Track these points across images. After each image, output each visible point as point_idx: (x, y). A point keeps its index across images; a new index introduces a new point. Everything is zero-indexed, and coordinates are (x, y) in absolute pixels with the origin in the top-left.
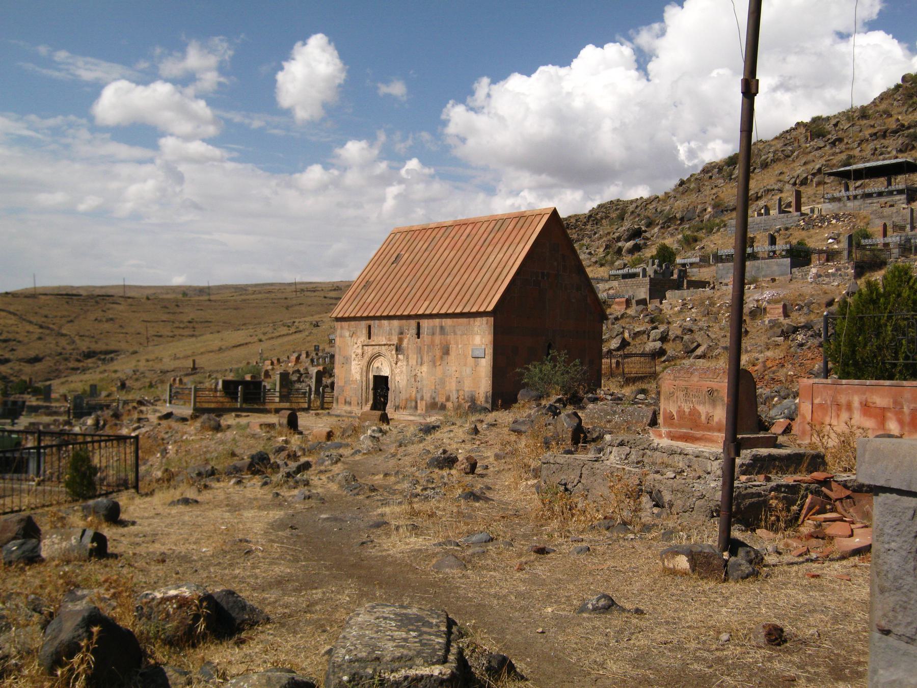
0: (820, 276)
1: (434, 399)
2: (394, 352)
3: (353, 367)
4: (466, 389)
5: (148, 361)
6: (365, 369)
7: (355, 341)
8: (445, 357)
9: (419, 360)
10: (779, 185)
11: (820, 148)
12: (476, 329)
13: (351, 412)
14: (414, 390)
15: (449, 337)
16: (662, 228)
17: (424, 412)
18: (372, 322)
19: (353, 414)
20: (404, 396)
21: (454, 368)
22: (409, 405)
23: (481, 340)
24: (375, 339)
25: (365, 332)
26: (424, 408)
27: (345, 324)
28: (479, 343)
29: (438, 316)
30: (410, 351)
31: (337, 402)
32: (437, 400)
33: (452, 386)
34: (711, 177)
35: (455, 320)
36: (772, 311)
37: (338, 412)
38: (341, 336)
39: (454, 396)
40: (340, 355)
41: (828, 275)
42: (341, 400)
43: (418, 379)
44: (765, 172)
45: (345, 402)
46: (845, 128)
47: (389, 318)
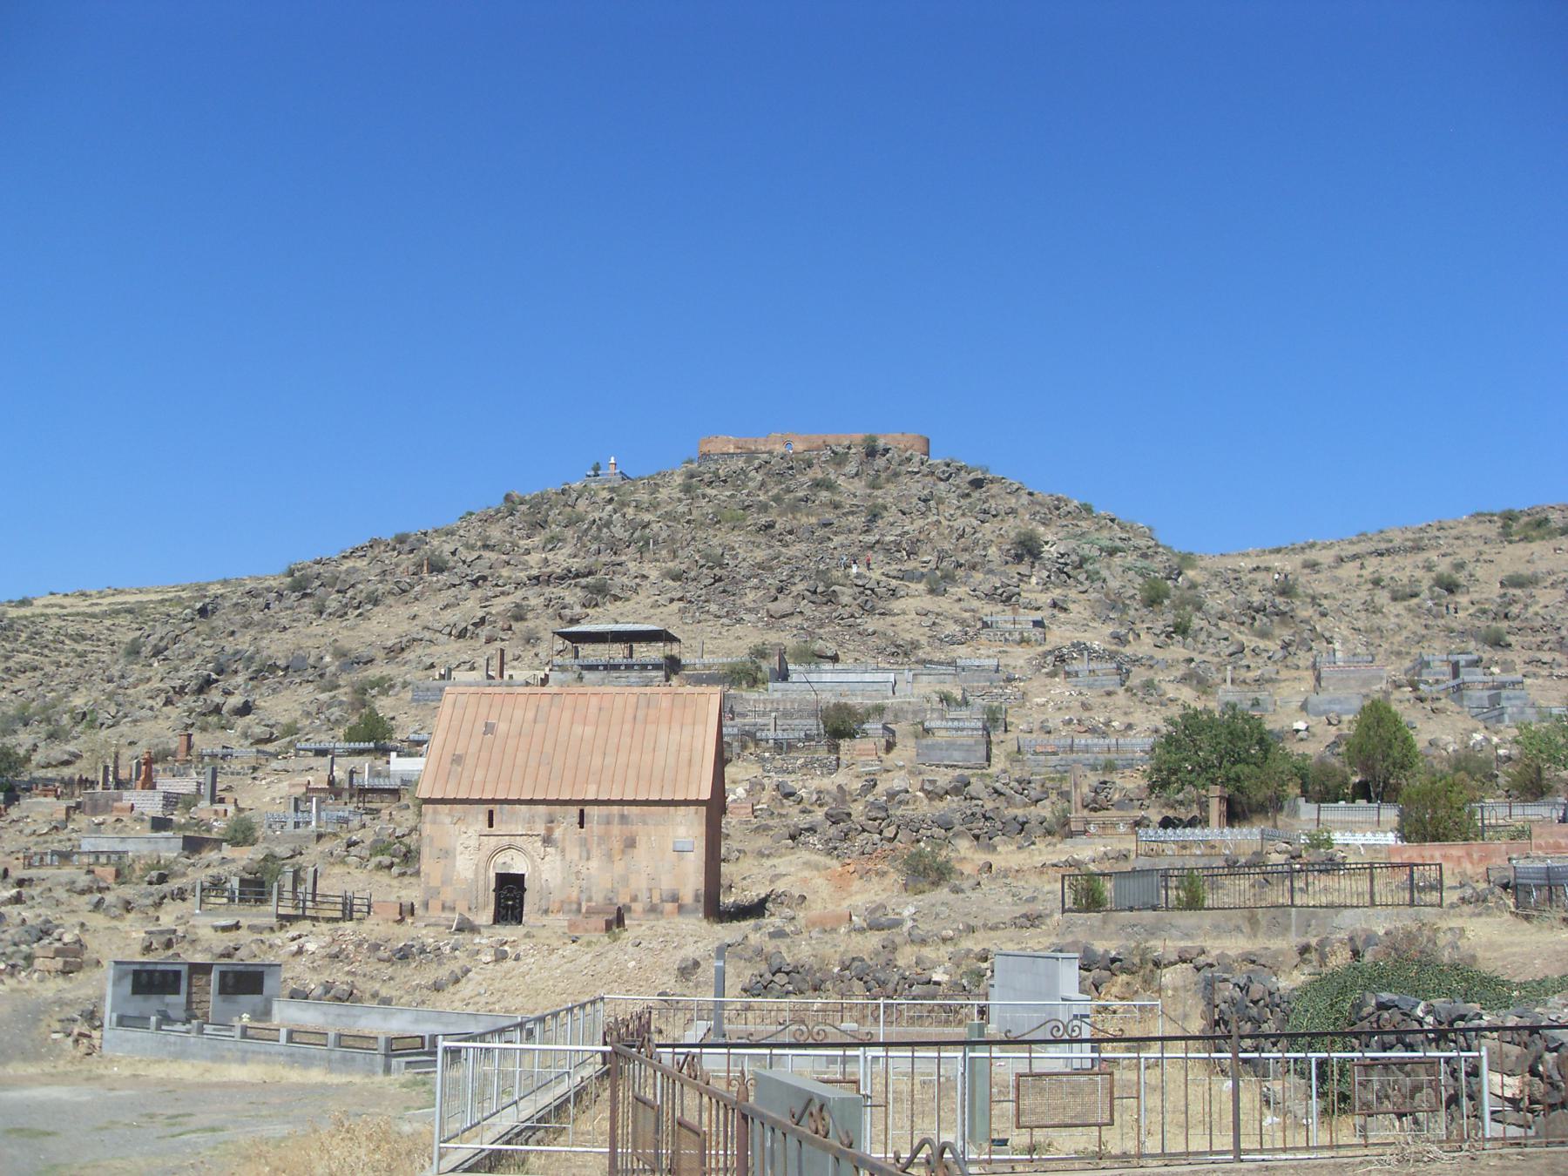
3: (457, 864)
6: (482, 864)
7: (464, 829)
8: (630, 850)
9: (584, 855)
10: (427, 635)
11: (454, 586)
12: (679, 819)
16: (251, 679)
20: (557, 897)
22: (566, 907)
25: (484, 818)
27: (445, 808)
29: (622, 803)
34: (267, 606)
36: (737, 811)
38: (434, 822)
39: (643, 896)
44: (376, 609)
45: (444, 908)
46: (469, 560)
47: (531, 802)
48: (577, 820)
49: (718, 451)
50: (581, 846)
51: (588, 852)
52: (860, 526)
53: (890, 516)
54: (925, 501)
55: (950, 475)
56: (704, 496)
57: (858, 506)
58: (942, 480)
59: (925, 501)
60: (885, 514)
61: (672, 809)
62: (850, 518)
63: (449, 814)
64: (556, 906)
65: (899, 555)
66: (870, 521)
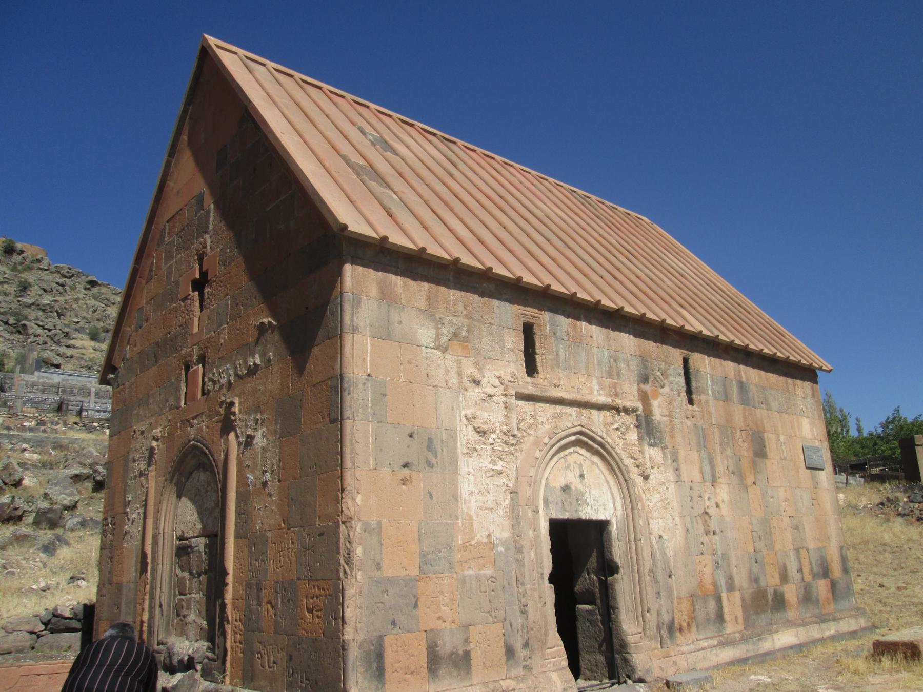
1: (756, 580)
2: (633, 436)
3: (466, 486)
4: (812, 545)
9: (707, 469)
14: (708, 559)
15: (758, 411)
17: (741, 627)
20: (682, 585)
21: (782, 494)
22: (700, 615)
26: (740, 620)
30: (679, 439)
33: (785, 540)
35: (763, 373)
38: (384, 333)
40: (380, 421)
43: (713, 525)
48: (681, 380)
51: (711, 462)
52: (12, 292)
53: (35, 291)
54: (62, 285)
55: (73, 276)
57: (11, 280)
58: (66, 277)
59: (62, 285)
60: (31, 289)
61: (789, 380)
62: (6, 286)
63: (429, 313)
65: (52, 314)
66: (21, 290)
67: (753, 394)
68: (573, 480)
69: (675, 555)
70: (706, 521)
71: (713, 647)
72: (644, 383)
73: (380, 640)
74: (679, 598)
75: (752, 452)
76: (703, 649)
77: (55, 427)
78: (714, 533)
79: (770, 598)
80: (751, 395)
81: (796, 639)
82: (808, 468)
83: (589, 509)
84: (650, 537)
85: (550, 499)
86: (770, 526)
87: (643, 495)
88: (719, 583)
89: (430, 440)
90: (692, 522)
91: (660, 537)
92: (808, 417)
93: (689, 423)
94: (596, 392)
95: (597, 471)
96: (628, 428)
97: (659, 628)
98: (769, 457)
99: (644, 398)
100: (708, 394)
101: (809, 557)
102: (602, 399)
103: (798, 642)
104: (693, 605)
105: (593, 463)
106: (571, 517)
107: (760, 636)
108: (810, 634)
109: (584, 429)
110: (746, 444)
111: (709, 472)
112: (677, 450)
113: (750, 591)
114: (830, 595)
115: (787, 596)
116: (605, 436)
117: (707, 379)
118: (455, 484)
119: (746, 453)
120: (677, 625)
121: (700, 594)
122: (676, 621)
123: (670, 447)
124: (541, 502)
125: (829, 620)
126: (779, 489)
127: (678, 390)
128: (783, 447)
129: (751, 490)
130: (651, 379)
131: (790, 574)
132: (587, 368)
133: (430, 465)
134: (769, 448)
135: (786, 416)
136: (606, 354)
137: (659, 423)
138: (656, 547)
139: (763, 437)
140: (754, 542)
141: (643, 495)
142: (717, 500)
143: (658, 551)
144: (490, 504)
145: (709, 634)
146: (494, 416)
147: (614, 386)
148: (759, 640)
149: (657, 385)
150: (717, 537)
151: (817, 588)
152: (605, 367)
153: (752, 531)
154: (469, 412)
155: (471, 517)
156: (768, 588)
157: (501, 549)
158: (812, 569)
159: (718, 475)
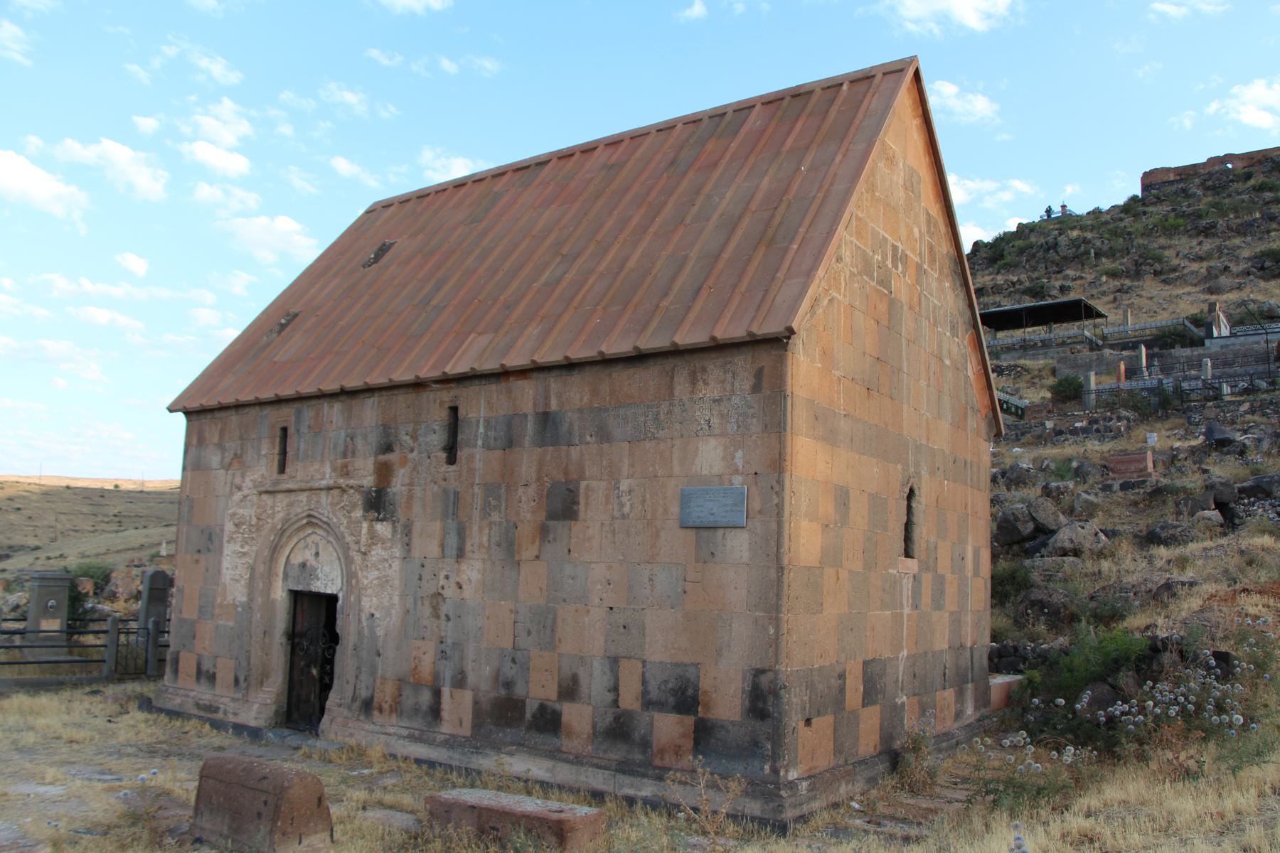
0: (1060, 433)
1: (508, 685)
2: (358, 513)
3: (226, 563)
5: (49, 558)
6: (261, 568)
7: (238, 480)
8: (559, 527)
9: (452, 541)
13: (212, 709)
15: (575, 452)
17: (466, 731)
18: (286, 415)
19: (220, 715)
20: (390, 666)
22: (408, 700)
23: (728, 458)
24: (299, 472)
25: (269, 450)
28: (718, 468)
30: (417, 508)
31: (176, 671)
32: (519, 691)
37: (175, 702)
39: (595, 683)
41: (1075, 432)
42: (188, 664)
43: (445, 609)
45: (199, 673)
48: (437, 439)
49: (1159, 181)
50: (445, 516)
51: (462, 534)
56: (1145, 213)
63: (221, 447)
64: (386, 694)
67: (571, 425)
68: (310, 557)
69: (386, 635)
70: (438, 603)
71: (400, 737)
72: (384, 454)
73: (178, 653)
74: (384, 679)
75: (544, 514)
76: (389, 734)
77: (1109, 424)
78: (448, 618)
79: (528, 715)
80: (565, 427)
81: (549, 775)
82: (684, 527)
83: (318, 584)
84: (359, 615)
85: (290, 574)
86: (554, 621)
87: (360, 572)
88: (442, 675)
89: (210, 534)
90: (415, 604)
91: (373, 615)
92: (723, 434)
93: (436, 488)
94: (328, 476)
95: (331, 549)
96: (354, 506)
97: (354, 699)
98: (582, 515)
99: (384, 472)
100: (475, 446)
101: (643, 674)
102: (324, 483)
103: (547, 779)
104: (399, 689)
105: (329, 542)
106: (304, 589)
107: (477, 751)
108: (583, 778)
109: (312, 513)
110: (535, 503)
111: (455, 546)
112: (413, 522)
113: (492, 695)
114: (690, 744)
115: (565, 718)
116: (331, 516)
117: (478, 426)
118: (220, 563)
119: (529, 516)
120: (375, 704)
121: (411, 680)
122: (376, 700)
123: (403, 520)
124: (281, 576)
125: (644, 776)
126: (593, 566)
127: (428, 451)
128: (625, 499)
129: (525, 569)
130: (397, 448)
131: (584, 688)
132: (322, 455)
133: (209, 550)
134: (587, 504)
135: (648, 444)
136: (343, 434)
137: (394, 494)
138: (365, 624)
139: (578, 488)
140: (515, 637)
141: (360, 572)
142: (458, 580)
143: (366, 628)
144: (237, 577)
145: (415, 725)
146: (248, 512)
147: (346, 466)
148: (472, 753)
149: (405, 450)
150: (450, 623)
151: (652, 724)
152: (341, 448)
153: (515, 622)
154: (230, 512)
155: (226, 585)
156: (528, 701)
157: (240, 609)
158: (645, 693)
159: (468, 547)
